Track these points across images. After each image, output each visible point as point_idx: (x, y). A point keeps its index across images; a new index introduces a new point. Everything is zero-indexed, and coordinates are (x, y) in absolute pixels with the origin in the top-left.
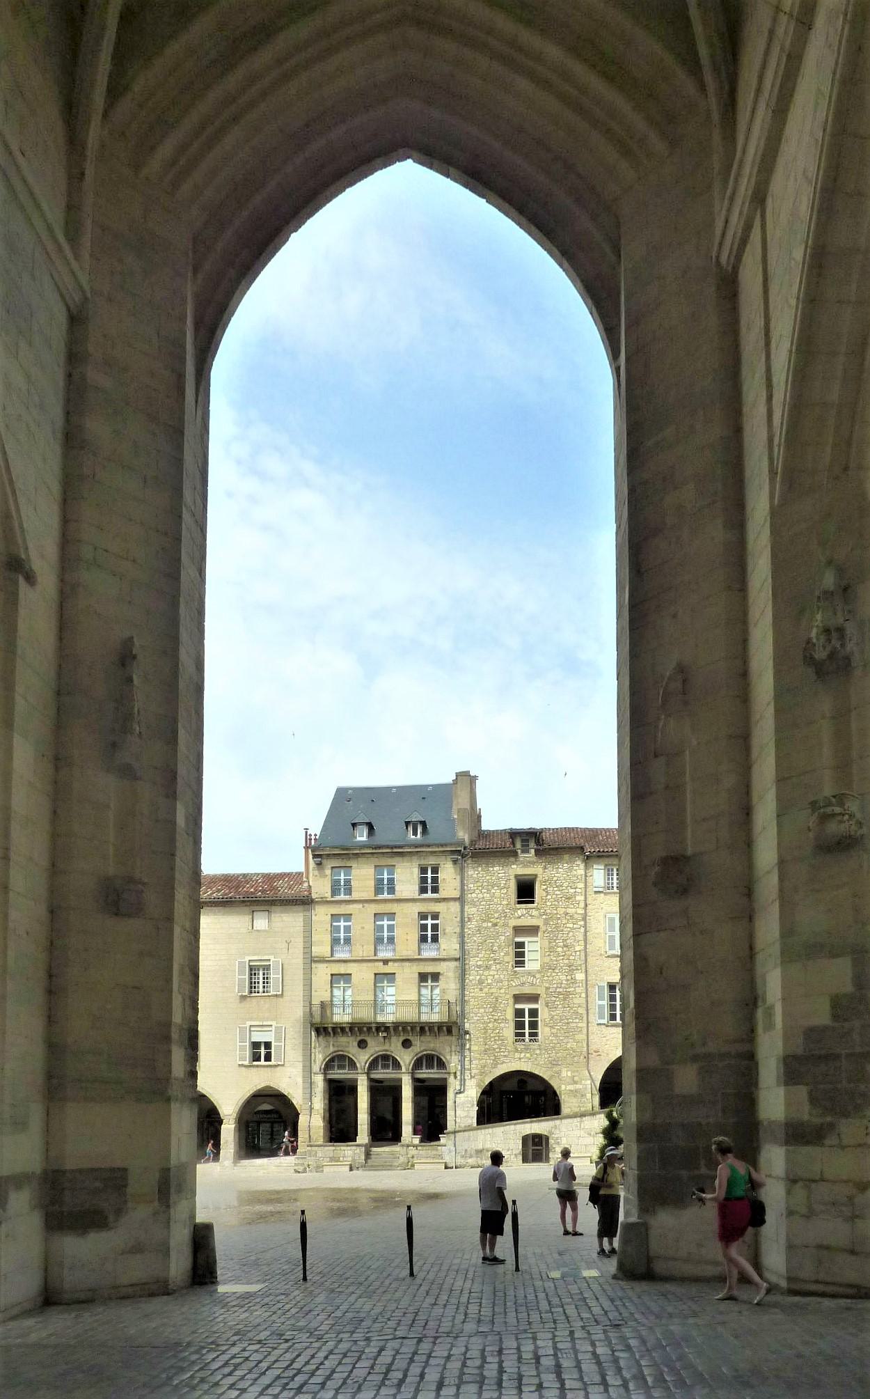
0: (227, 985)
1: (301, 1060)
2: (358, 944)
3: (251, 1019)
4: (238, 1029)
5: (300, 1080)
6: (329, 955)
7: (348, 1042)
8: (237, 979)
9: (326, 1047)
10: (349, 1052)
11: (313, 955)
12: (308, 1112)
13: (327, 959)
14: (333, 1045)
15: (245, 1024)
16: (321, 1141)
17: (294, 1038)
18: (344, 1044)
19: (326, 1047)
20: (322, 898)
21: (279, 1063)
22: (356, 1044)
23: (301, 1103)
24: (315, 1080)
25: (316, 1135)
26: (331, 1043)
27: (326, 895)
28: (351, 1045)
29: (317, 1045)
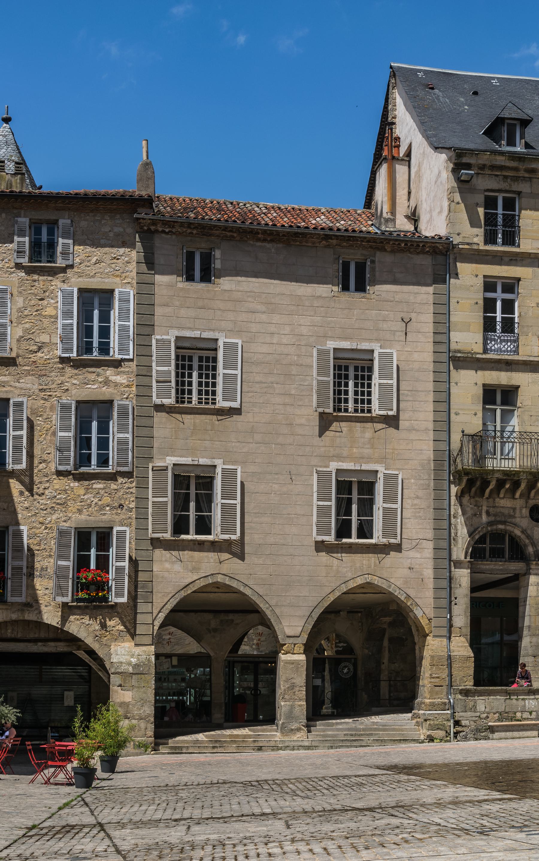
0: (293, 392)
1: (430, 534)
2: (530, 334)
3: (339, 458)
4: (315, 476)
5: (429, 573)
6: (479, 348)
7: (514, 509)
8: (315, 383)
9: (475, 515)
10: (515, 525)
11: (453, 346)
12: (444, 632)
13: (478, 356)
14: (488, 513)
15: (327, 466)
16: (469, 684)
17: (418, 497)
18: (506, 512)
19: (475, 515)
20: (468, 244)
21: (392, 541)
22: (525, 512)
23: (432, 616)
24: (457, 576)
25: (462, 674)
26: (485, 508)
27: (476, 240)
28: (518, 514)
29: (460, 511)
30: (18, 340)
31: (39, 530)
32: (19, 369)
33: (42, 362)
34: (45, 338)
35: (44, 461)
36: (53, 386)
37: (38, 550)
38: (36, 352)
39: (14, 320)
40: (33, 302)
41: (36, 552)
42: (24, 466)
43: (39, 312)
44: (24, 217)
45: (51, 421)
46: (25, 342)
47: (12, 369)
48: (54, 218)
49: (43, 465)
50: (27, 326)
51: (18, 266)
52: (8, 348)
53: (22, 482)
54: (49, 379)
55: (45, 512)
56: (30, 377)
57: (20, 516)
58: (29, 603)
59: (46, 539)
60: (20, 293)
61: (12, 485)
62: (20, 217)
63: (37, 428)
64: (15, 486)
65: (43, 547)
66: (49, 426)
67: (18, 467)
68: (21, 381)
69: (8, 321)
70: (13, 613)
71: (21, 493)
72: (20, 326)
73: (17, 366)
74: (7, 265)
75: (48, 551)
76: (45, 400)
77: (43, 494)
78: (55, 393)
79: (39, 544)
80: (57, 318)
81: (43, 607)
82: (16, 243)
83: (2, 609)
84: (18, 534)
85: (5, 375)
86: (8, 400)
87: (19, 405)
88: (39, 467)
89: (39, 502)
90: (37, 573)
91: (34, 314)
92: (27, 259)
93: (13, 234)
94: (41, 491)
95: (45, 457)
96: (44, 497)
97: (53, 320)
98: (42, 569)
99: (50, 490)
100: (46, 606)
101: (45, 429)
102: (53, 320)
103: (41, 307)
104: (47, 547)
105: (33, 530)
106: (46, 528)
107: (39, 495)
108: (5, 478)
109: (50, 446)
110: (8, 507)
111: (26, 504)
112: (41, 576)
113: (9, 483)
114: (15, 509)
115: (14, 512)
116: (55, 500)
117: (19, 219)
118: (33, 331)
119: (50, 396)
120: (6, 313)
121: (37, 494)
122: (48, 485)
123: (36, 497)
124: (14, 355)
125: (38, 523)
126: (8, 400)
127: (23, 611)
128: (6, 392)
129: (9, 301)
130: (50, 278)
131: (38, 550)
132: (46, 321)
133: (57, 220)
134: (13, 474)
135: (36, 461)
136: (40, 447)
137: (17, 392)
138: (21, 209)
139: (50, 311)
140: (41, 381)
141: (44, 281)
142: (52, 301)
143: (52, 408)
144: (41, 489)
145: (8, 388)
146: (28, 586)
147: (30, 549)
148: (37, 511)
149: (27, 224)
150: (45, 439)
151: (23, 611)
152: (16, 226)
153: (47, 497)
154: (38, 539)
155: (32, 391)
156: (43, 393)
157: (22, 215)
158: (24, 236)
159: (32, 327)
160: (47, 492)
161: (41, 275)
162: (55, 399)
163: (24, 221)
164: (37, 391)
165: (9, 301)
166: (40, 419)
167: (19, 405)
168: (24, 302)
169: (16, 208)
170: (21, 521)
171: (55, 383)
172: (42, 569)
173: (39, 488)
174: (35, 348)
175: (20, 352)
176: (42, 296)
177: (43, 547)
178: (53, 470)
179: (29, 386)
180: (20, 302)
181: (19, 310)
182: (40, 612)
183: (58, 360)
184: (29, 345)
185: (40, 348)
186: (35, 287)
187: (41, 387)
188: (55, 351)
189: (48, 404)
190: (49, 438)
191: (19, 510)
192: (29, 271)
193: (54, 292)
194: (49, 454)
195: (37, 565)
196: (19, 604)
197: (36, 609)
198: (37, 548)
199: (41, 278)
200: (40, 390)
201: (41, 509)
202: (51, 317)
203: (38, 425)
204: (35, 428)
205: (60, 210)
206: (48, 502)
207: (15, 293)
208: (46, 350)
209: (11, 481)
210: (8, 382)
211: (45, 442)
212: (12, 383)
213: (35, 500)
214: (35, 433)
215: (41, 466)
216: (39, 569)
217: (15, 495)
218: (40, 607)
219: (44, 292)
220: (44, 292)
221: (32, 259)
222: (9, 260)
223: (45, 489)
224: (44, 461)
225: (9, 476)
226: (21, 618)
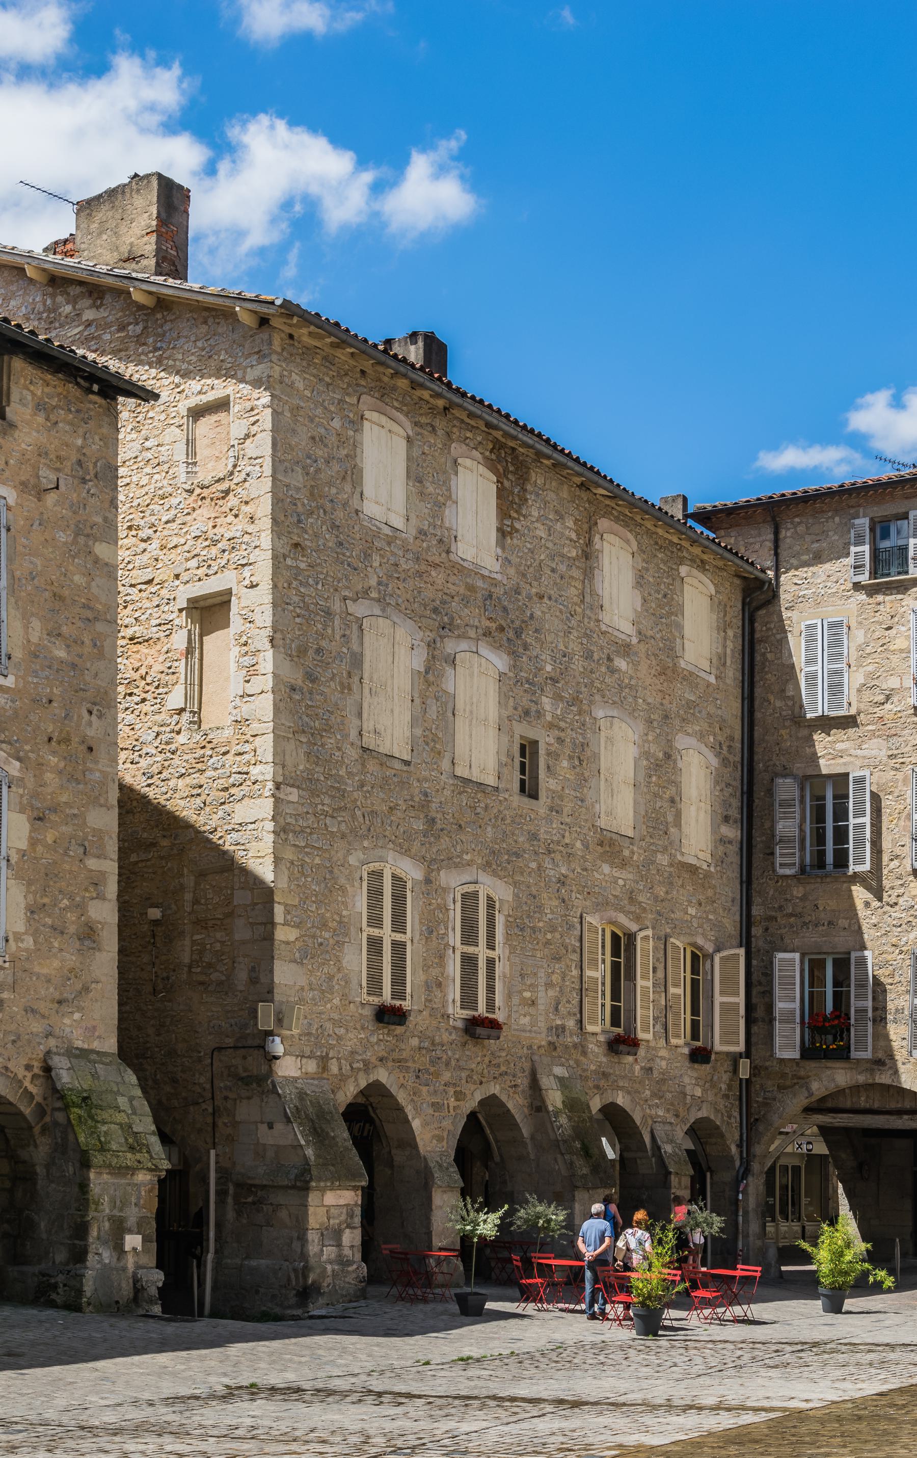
30: (859, 691)
31: (892, 956)
32: (860, 731)
33: (891, 716)
34: (893, 682)
35: (897, 857)
36: (907, 749)
37: (892, 984)
38: (883, 704)
39: (853, 663)
40: (877, 633)
41: (888, 987)
42: (866, 867)
43: (885, 647)
44: (864, 517)
45: (905, 800)
46: (868, 692)
47: (851, 731)
48: (904, 510)
49: (896, 863)
50: (870, 668)
51: (857, 586)
52: (845, 703)
53: (869, 888)
54: (901, 739)
55: (899, 929)
56: (876, 740)
57: (866, 936)
58: (880, 1060)
59: (901, 968)
60: (861, 623)
61: (855, 894)
62: (858, 518)
63: (885, 812)
64: (860, 894)
65: (897, 979)
66: (902, 807)
67: (860, 868)
68: (863, 747)
69: (844, 665)
70: (859, 1073)
71: (867, 904)
72: (861, 670)
73: (858, 727)
74: (843, 587)
75: (905, 984)
76: (896, 769)
77: (896, 904)
78: (909, 759)
79: (892, 975)
80: (909, 652)
81: (900, 1065)
82: (852, 554)
83: (845, 1068)
84: (862, 962)
85: (843, 741)
86: (847, 775)
87: (860, 781)
88: (889, 866)
89: (890, 916)
90: (890, 1017)
91: (879, 650)
92: (867, 574)
93: (849, 544)
94: (893, 900)
95: (898, 851)
96: (897, 908)
97: (904, 655)
98: (897, 1010)
99: (905, 898)
100: (904, 1064)
101: (897, 811)
102: (904, 655)
103: (888, 640)
104: (903, 980)
105: (884, 956)
106: (901, 952)
107: (891, 906)
108: (845, 885)
109: (905, 835)
110: (850, 925)
111: (874, 920)
112: (895, 1021)
113: (851, 891)
114: (860, 928)
115: (859, 931)
116: (912, 912)
117: (857, 521)
118: (878, 674)
119: (903, 763)
120: (841, 654)
121: (888, 904)
122: (902, 891)
123: (888, 908)
124: (853, 711)
125: (889, 945)
126: (847, 775)
127: (872, 1071)
128: (845, 764)
129: (845, 637)
130: (899, 597)
131: (892, 984)
132: (895, 659)
133: (907, 513)
134: (857, 878)
135: (885, 858)
136: (890, 838)
137: (858, 763)
138: (859, 506)
139: (900, 643)
140: (890, 745)
141: (892, 602)
142: (903, 629)
143: (905, 780)
144: (893, 897)
145: (846, 759)
146: (876, 1036)
147: (877, 982)
148: (888, 929)
149: (867, 525)
150: (897, 825)
151: (872, 1071)
152: (852, 531)
153: (902, 908)
154: (891, 968)
155: (879, 759)
156: (894, 761)
157: (861, 514)
158: (863, 543)
159: (877, 670)
160: (901, 900)
161: (887, 595)
162: (910, 766)
163: (863, 523)
164: (885, 759)
165: (845, 637)
166: (890, 797)
167: (860, 781)
168: (865, 636)
169: (853, 507)
170: (868, 944)
171: (910, 744)
172: (897, 1010)
173: (890, 896)
174: (881, 698)
175: (862, 707)
176: (889, 623)
177: (897, 979)
178: (909, 869)
179: (874, 753)
180: (859, 636)
181: (860, 649)
182: (896, 1072)
183: (912, 711)
184: (874, 694)
185: (888, 698)
186: (879, 613)
187: (890, 753)
188: (909, 699)
189: (900, 776)
190: (902, 823)
191: (865, 928)
192: (872, 590)
193: (906, 615)
194: (903, 846)
195: (890, 1006)
196: (867, 1060)
197: (891, 1068)
198: (890, 981)
199: (888, 598)
200: (890, 756)
201: (894, 926)
202: (901, 651)
203: (888, 807)
204: (883, 810)
205: (910, 498)
206: (903, 915)
207: (853, 625)
208: (895, 699)
209: (853, 888)
210: (846, 750)
211: (897, 829)
212: (853, 752)
213: (885, 913)
214: (883, 818)
215: (893, 864)
216: (893, 1011)
217: (858, 908)
218: (896, 1065)
219: (892, 617)
220: (892, 617)
221: (876, 573)
222: (845, 580)
223: (898, 896)
224: (897, 857)
225: (850, 882)
226: (870, 1081)
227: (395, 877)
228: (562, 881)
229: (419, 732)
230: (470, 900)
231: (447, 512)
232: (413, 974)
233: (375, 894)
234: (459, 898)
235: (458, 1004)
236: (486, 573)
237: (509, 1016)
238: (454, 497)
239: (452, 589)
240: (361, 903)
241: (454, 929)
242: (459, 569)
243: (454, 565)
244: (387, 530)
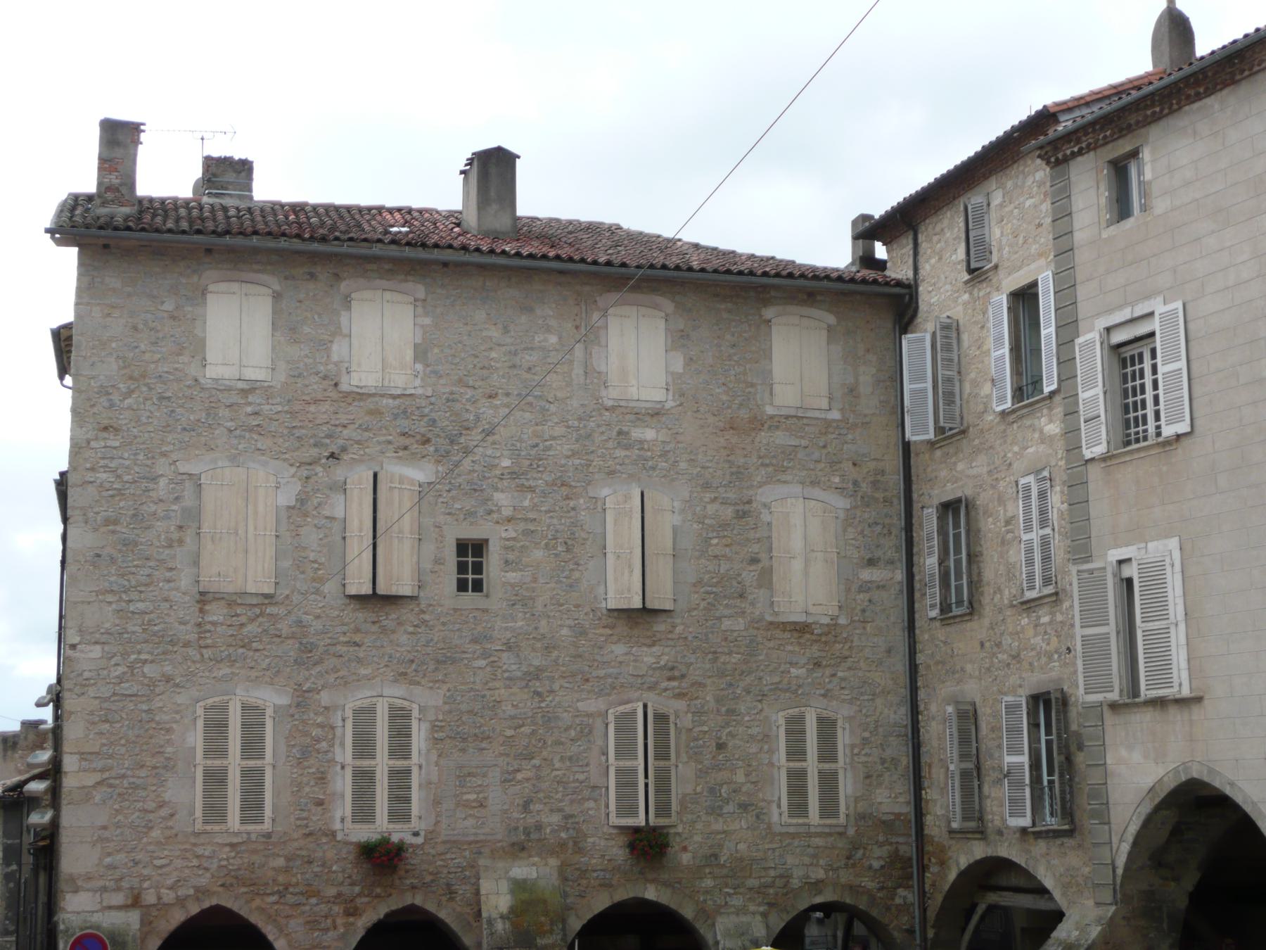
227: (245, 708)
228: (536, 674)
229: (287, 564)
230: (365, 716)
231: (335, 347)
232: (276, 794)
233: (216, 727)
234: (349, 713)
235: (349, 819)
236: (399, 392)
237: (437, 823)
238: (345, 331)
239: (343, 419)
240: (196, 739)
241: (342, 745)
242: (360, 396)
243: (347, 395)
244: (241, 385)
